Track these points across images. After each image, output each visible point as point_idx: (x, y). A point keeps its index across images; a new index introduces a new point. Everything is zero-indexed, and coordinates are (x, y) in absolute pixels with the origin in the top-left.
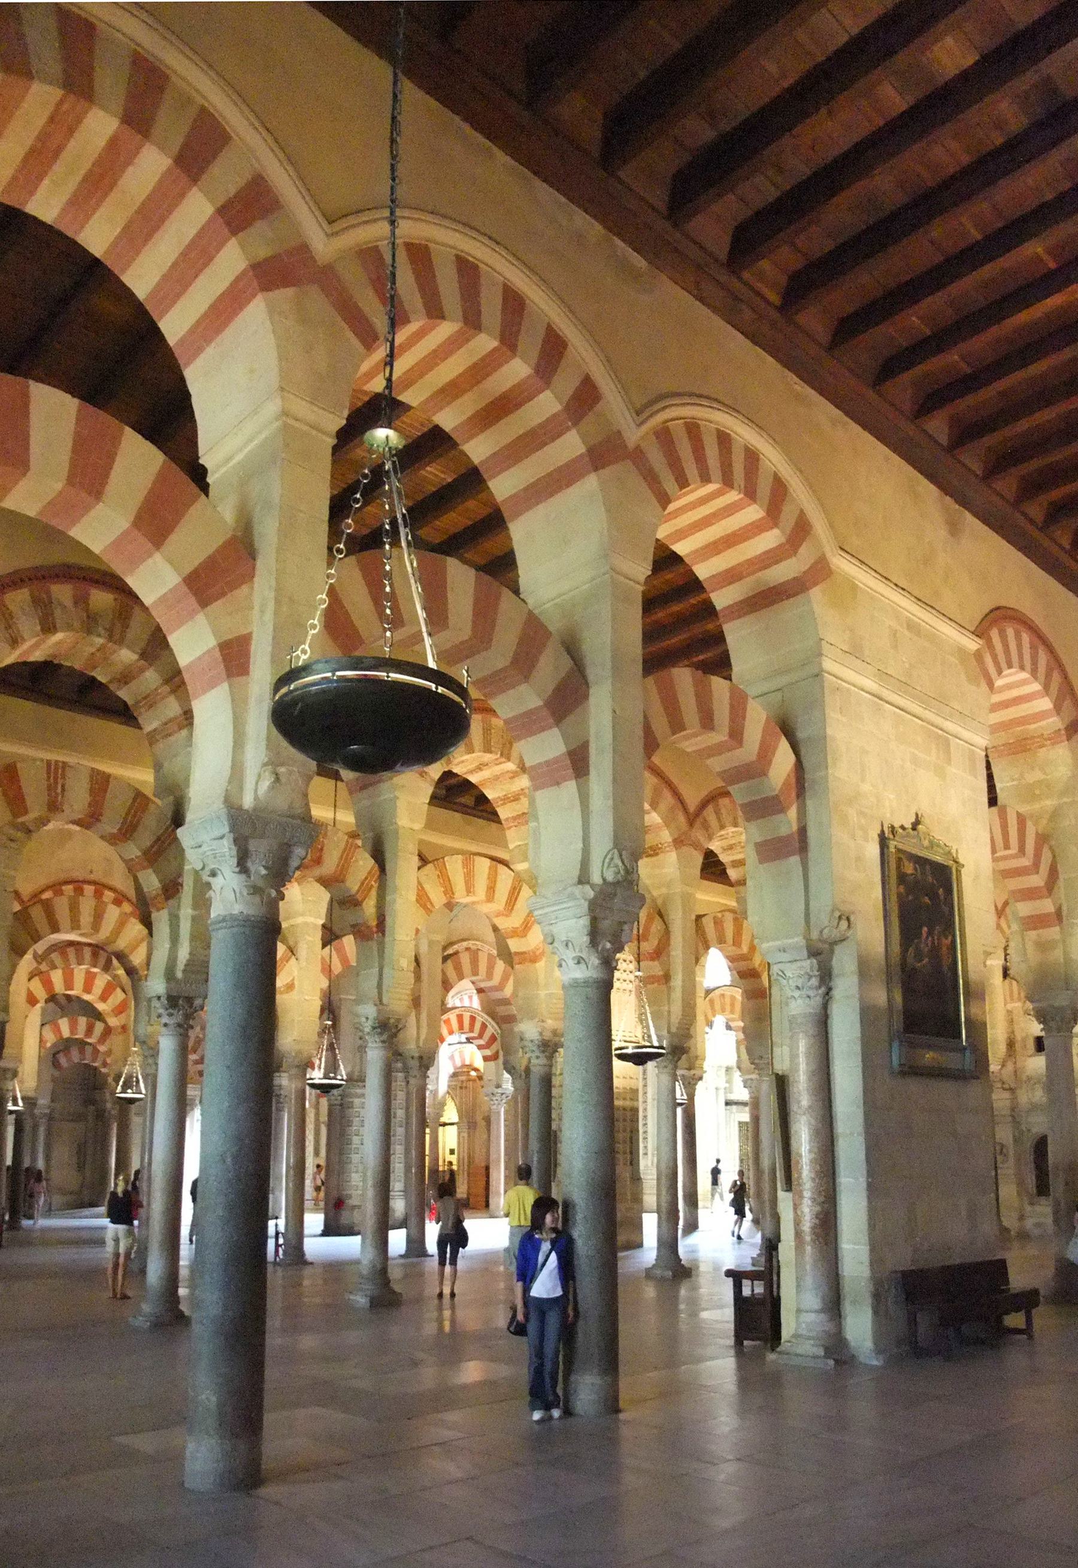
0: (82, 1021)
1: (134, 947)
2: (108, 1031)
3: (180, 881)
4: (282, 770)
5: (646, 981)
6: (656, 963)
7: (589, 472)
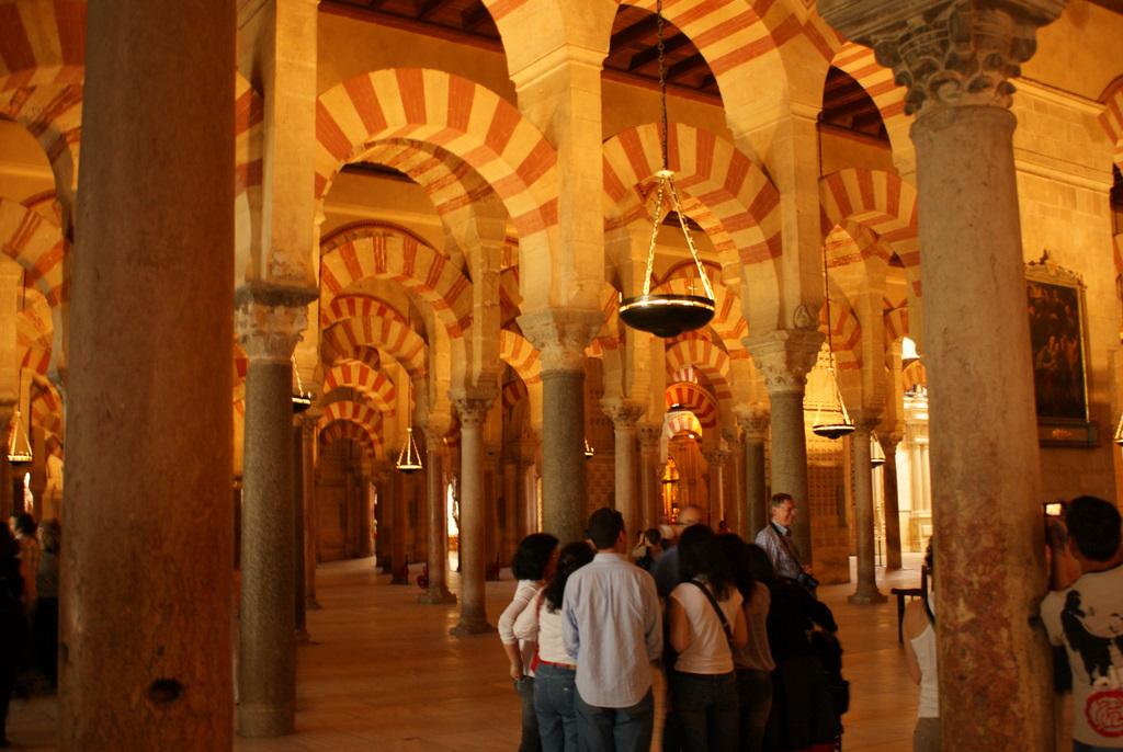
0: (350, 406)
1: (414, 352)
2: (371, 412)
3: (471, 315)
4: (583, 282)
5: (842, 366)
6: (850, 352)
7: (772, 48)
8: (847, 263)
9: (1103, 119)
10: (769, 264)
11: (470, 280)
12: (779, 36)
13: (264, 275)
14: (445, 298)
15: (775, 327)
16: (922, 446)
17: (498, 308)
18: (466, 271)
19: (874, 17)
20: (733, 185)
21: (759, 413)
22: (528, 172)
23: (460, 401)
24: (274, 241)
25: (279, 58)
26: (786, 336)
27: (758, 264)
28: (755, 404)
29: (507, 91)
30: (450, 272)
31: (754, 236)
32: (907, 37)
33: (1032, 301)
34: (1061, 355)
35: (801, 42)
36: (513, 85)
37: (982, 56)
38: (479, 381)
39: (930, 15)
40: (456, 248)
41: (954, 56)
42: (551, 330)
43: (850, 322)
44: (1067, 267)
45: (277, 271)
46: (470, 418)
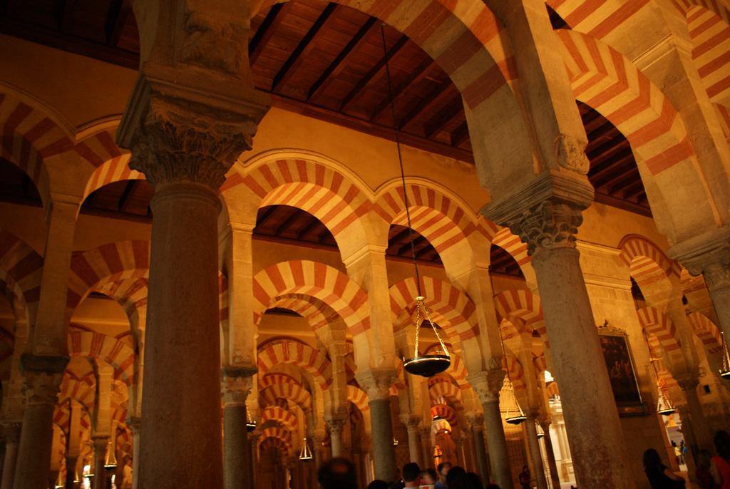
0: (274, 429)
2: (285, 432)
4: (386, 355)
5: (516, 388)
7: (463, 238)
8: (512, 337)
9: (621, 256)
10: (474, 340)
11: (330, 361)
12: (467, 232)
13: (231, 363)
14: (319, 370)
15: (481, 369)
16: (562, 425)
17: (345, 374)
18: (328, 357)
19: (507, 213)
20: (452, 303)
21: (478, 416)
22: (355, 305)
23: (329, 421)
24: (235, 345)
25: (235, 260)
26: (487, 374)
27: (468, 340)
28: (476, 411)
29: (341, 267)
30: (320, 358)
31: (465, 326)
32: (523, 220)
33: (603, 345)
34: (622, 370)
35: (477, 234)
36: (344, 265)
37: (559, 225)
38: (338, 411)
39: (533, 209)
40: (323, 346)
41: (546, 227)
42: (371, 380)
43: (517, 366)
44: (617, 327)
45: (237, 360)
46: (335, 429)
